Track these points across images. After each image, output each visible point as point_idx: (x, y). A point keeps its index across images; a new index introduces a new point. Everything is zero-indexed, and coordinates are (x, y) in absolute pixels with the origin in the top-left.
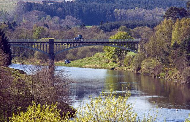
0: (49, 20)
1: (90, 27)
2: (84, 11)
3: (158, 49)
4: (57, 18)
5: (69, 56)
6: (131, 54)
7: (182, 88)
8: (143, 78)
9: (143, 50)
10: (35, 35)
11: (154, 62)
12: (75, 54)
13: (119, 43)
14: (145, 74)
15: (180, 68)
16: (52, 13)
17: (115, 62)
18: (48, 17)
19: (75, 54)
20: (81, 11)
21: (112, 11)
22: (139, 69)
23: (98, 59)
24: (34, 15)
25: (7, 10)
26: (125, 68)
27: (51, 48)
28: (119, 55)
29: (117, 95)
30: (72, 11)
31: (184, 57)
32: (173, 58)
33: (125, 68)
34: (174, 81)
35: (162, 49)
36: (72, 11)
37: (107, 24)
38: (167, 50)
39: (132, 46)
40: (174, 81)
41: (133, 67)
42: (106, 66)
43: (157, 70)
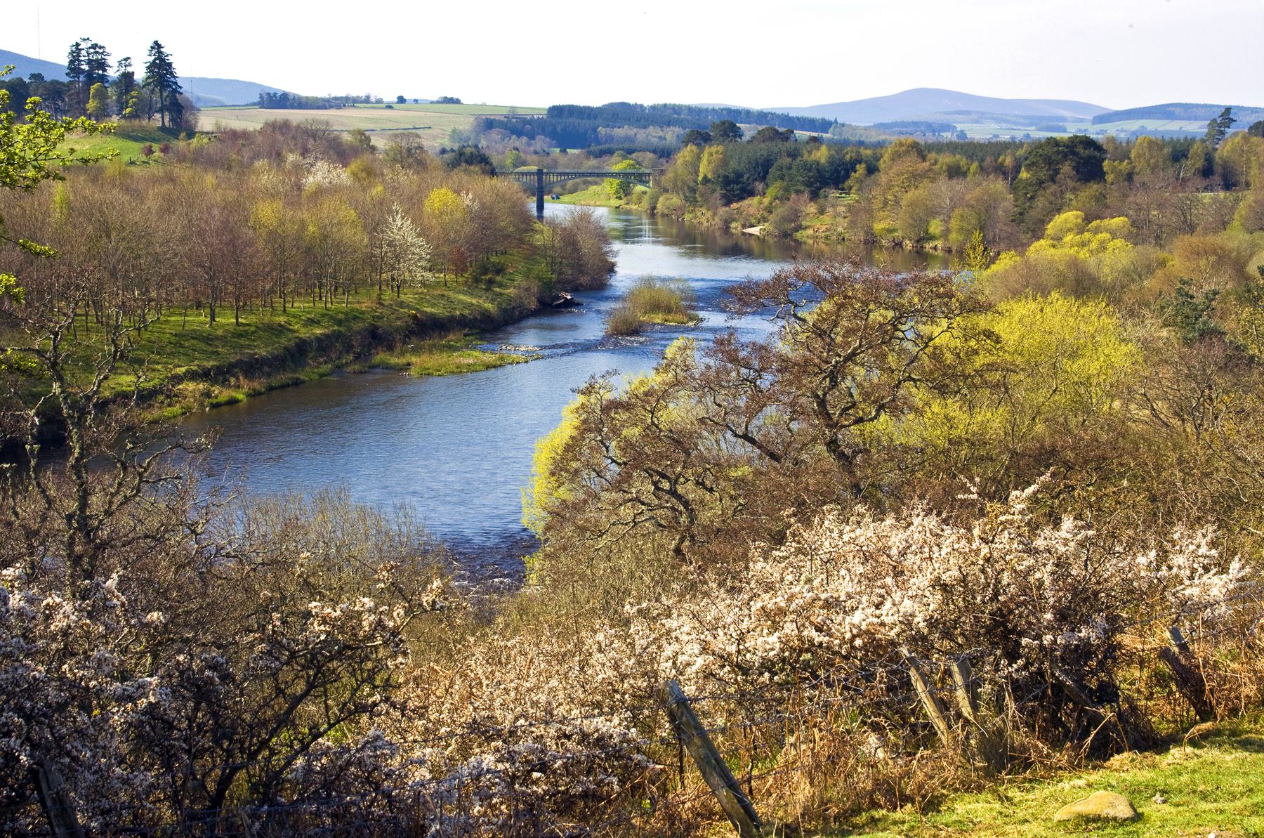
0: (515, 141)
1: (576, 151)
2: (559, 129)
3: (679, 184)
4: (525, 139)
5: (557, 189)
6: (639, 188)
7: (717, 234)
8: (659, 220)
9: (657, 183)
10: (509, 162)
11: (676, 200)
12: (563, 187)
13: (626, 175)
14: (663, 215)
15: (714, 209)
16: (519, 134)
17: (620, 198)
18: (514, 137)
19: (563, 187)
20: (555, 129)
21: (595, 130)
22: (654, 208)
23: (595, 194)
24: (495, 135)
25: (461, 128)
26: (634, 207)
27: (540, 180)
28: (624, 190)
29: (654, 242)
30: (543, 130)
31: (717, 195)
32: (702, 195)
33: (634, 207)
34: (705, 224)
35: (684, 183)
36: (543, 130)
37: (594, 148)
38: (692, 184)
39: (641, 178)
40: (705, 224)
41: (645, 205)
42: (608, 203)
43: (680, 210)
